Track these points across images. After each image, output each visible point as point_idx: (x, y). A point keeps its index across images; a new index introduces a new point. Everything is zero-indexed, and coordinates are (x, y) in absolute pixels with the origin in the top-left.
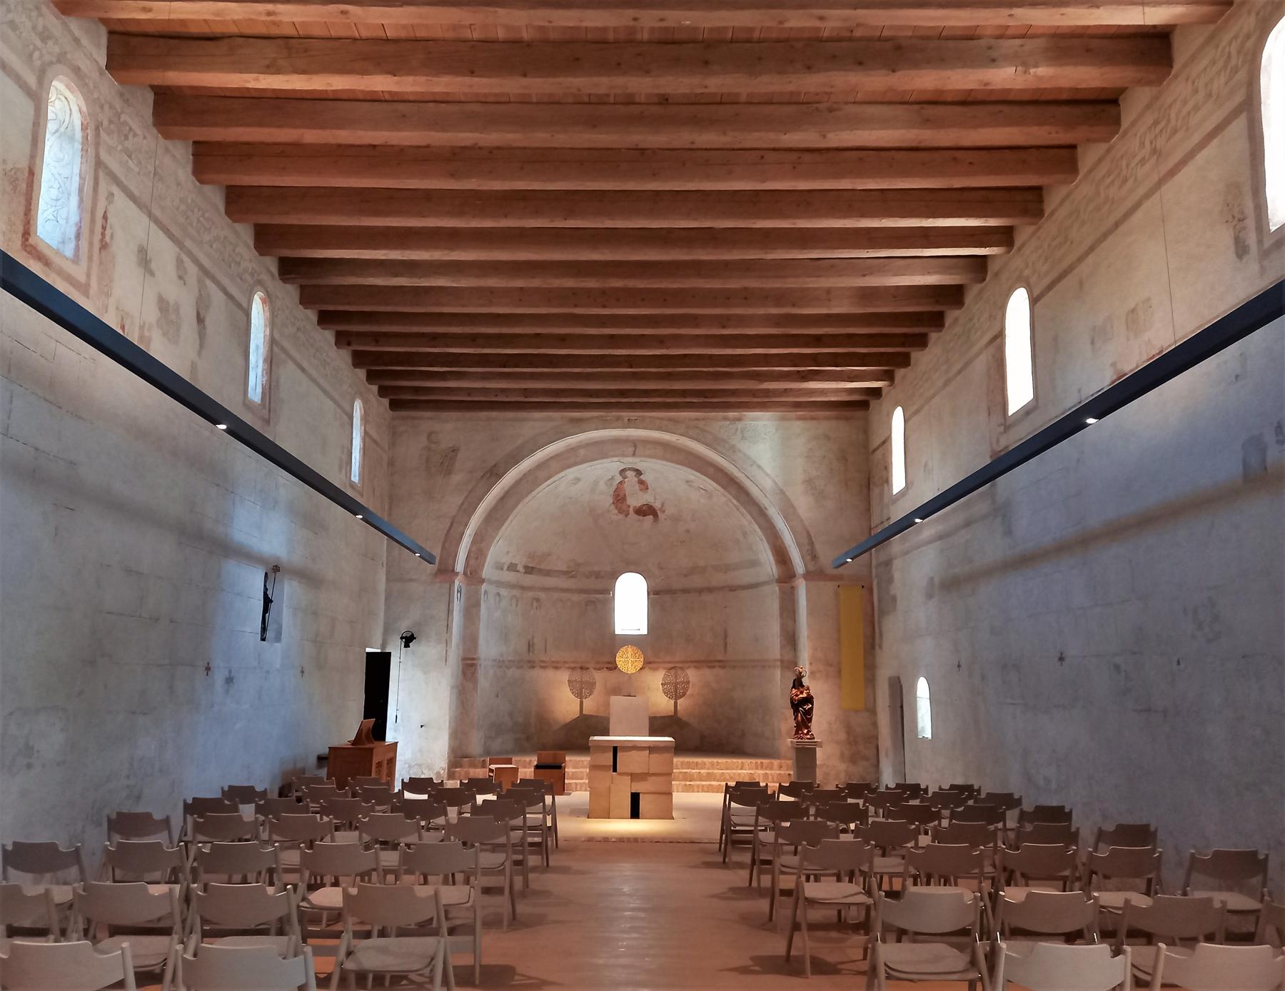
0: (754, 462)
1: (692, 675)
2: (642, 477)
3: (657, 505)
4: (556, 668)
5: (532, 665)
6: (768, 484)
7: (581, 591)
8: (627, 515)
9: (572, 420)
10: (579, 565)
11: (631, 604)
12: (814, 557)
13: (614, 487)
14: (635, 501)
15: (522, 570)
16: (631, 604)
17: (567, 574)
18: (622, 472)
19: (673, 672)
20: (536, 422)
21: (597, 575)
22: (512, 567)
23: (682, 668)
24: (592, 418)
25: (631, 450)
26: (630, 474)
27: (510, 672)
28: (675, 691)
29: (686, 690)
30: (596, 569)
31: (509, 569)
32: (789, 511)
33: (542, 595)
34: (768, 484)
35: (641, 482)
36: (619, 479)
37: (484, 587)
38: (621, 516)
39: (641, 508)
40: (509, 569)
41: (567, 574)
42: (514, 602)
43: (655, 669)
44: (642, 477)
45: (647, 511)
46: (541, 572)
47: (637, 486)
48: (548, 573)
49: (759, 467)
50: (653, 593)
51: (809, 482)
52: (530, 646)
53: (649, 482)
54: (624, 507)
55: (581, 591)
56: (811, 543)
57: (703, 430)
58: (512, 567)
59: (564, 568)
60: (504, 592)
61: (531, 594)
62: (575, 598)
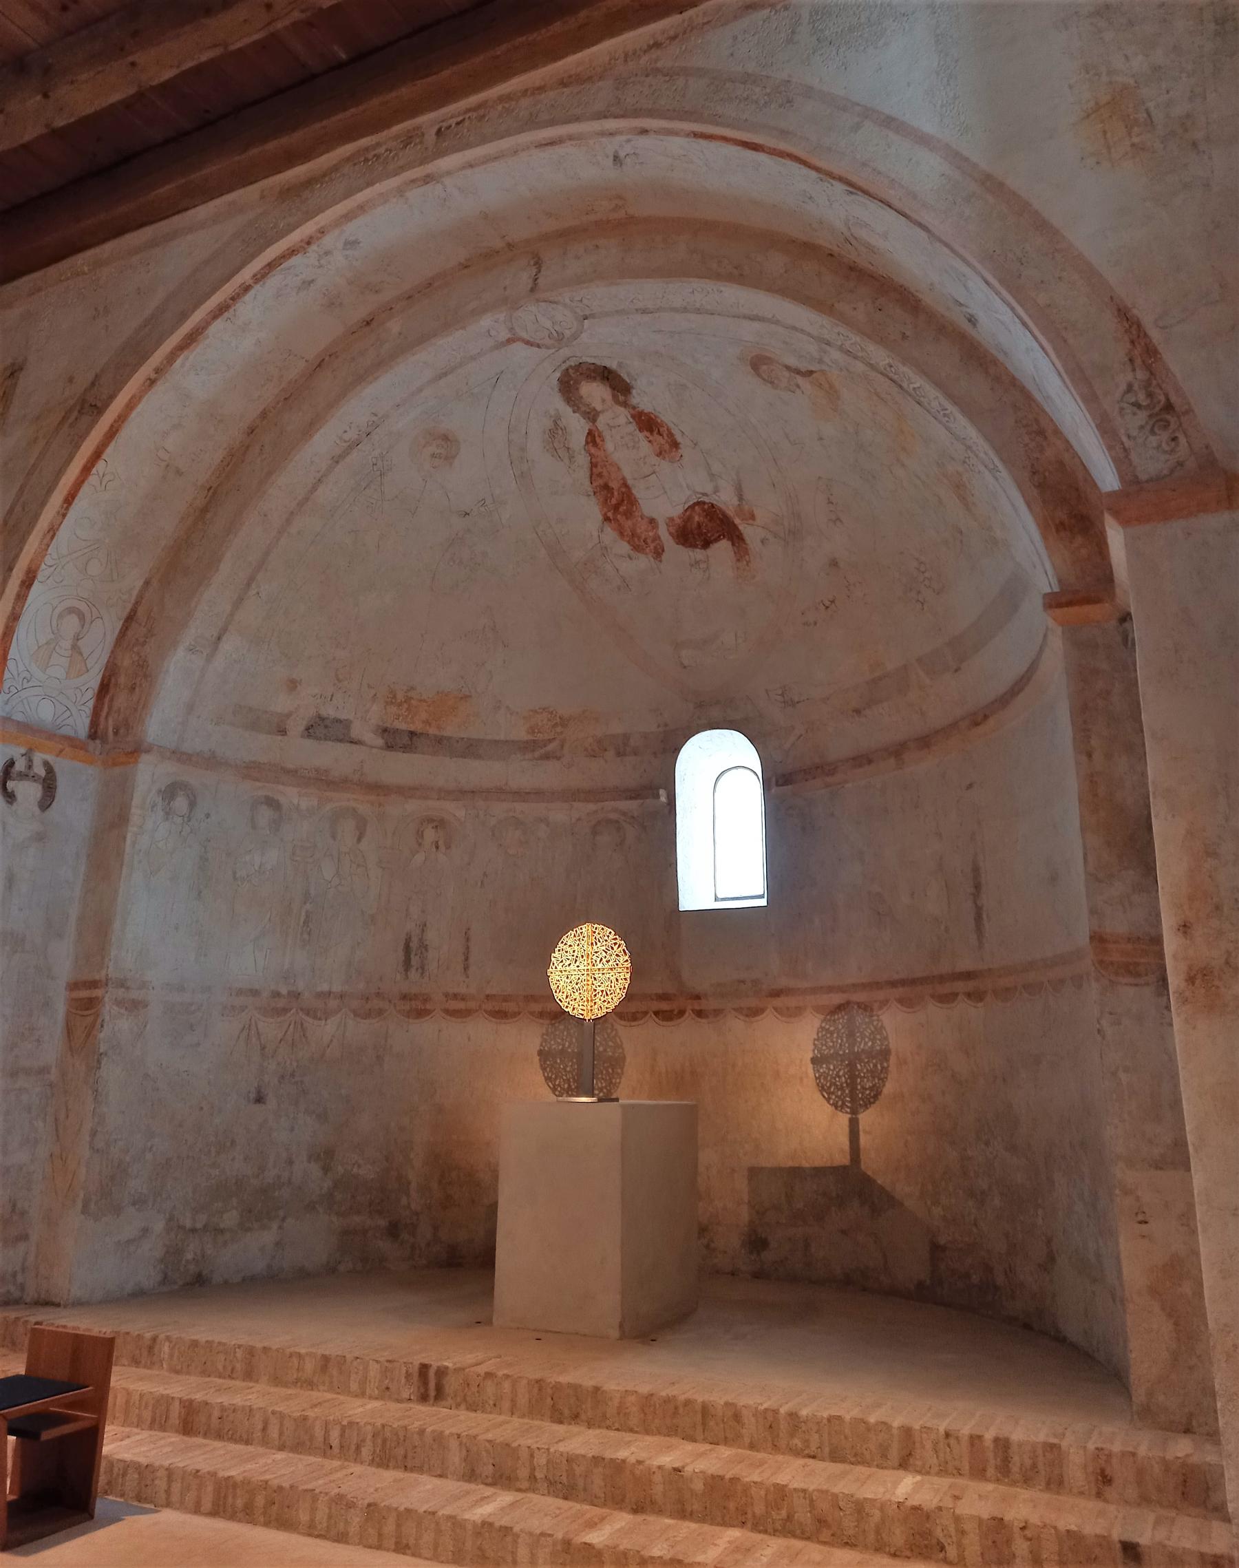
0: (868, 113)
1: (895, 1026)
2: (643, 399)
3: (726, 499)
4: (501, 1015)
5: (417, 1006)
6: (924, 173)
7: (572, 795)
8: (658, 553)
9: (289, 193)
10: (564, 722)
11: (721, 830)
12: (1165, 412)
13: (583, 460)
14: (664, 496)
15: (369, 737)
16: (721, 830)
17: (534, 747)
18: (568, 386)
19: (842, 1019)
20: (198, 233)
21: (622, 747)
22: (321, 728)
23: (866, 1007)
24: (335, 168)
25: (525, 278)
26: (594, 392)
27: (330, 1028)
28: (852, 1087)
29: (880, 1075)
30: (617, 728)
31: (309, 731)
32: (1021, 239)
33: (455, 810)
34: (924, 173)
35: (647, 423)
36: (577, 426)
37: (148, 775)
38: (644, 561)
39: (686, 519)
40: (309, 731)
41: (534, 747)
42: (348, 827)
43: (793, 1013)
44: (643, 399)
45: (707, 527)
46: (441, 744)
47: (644, 445)
48: (470, 749)
49: (889, 122)
50: (779, 782)
51: (1118, 112)
52: (411, 953)
53: (667, 417)
54: (642, 528)
55: (572, 795)
56: (1143, 352)
57: (670, 74)
58: (321, 728)
59: (522, 734)
60: (290, 795)
61: (413, 806)
62: (559, 814)
